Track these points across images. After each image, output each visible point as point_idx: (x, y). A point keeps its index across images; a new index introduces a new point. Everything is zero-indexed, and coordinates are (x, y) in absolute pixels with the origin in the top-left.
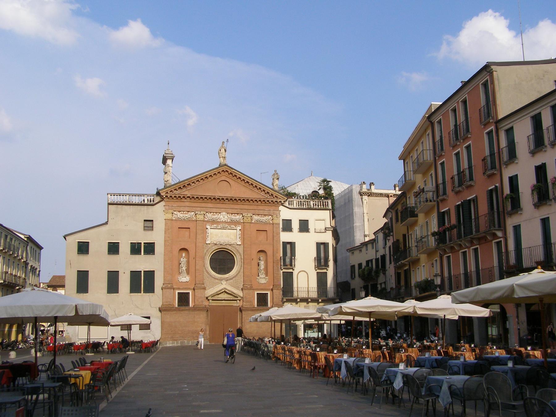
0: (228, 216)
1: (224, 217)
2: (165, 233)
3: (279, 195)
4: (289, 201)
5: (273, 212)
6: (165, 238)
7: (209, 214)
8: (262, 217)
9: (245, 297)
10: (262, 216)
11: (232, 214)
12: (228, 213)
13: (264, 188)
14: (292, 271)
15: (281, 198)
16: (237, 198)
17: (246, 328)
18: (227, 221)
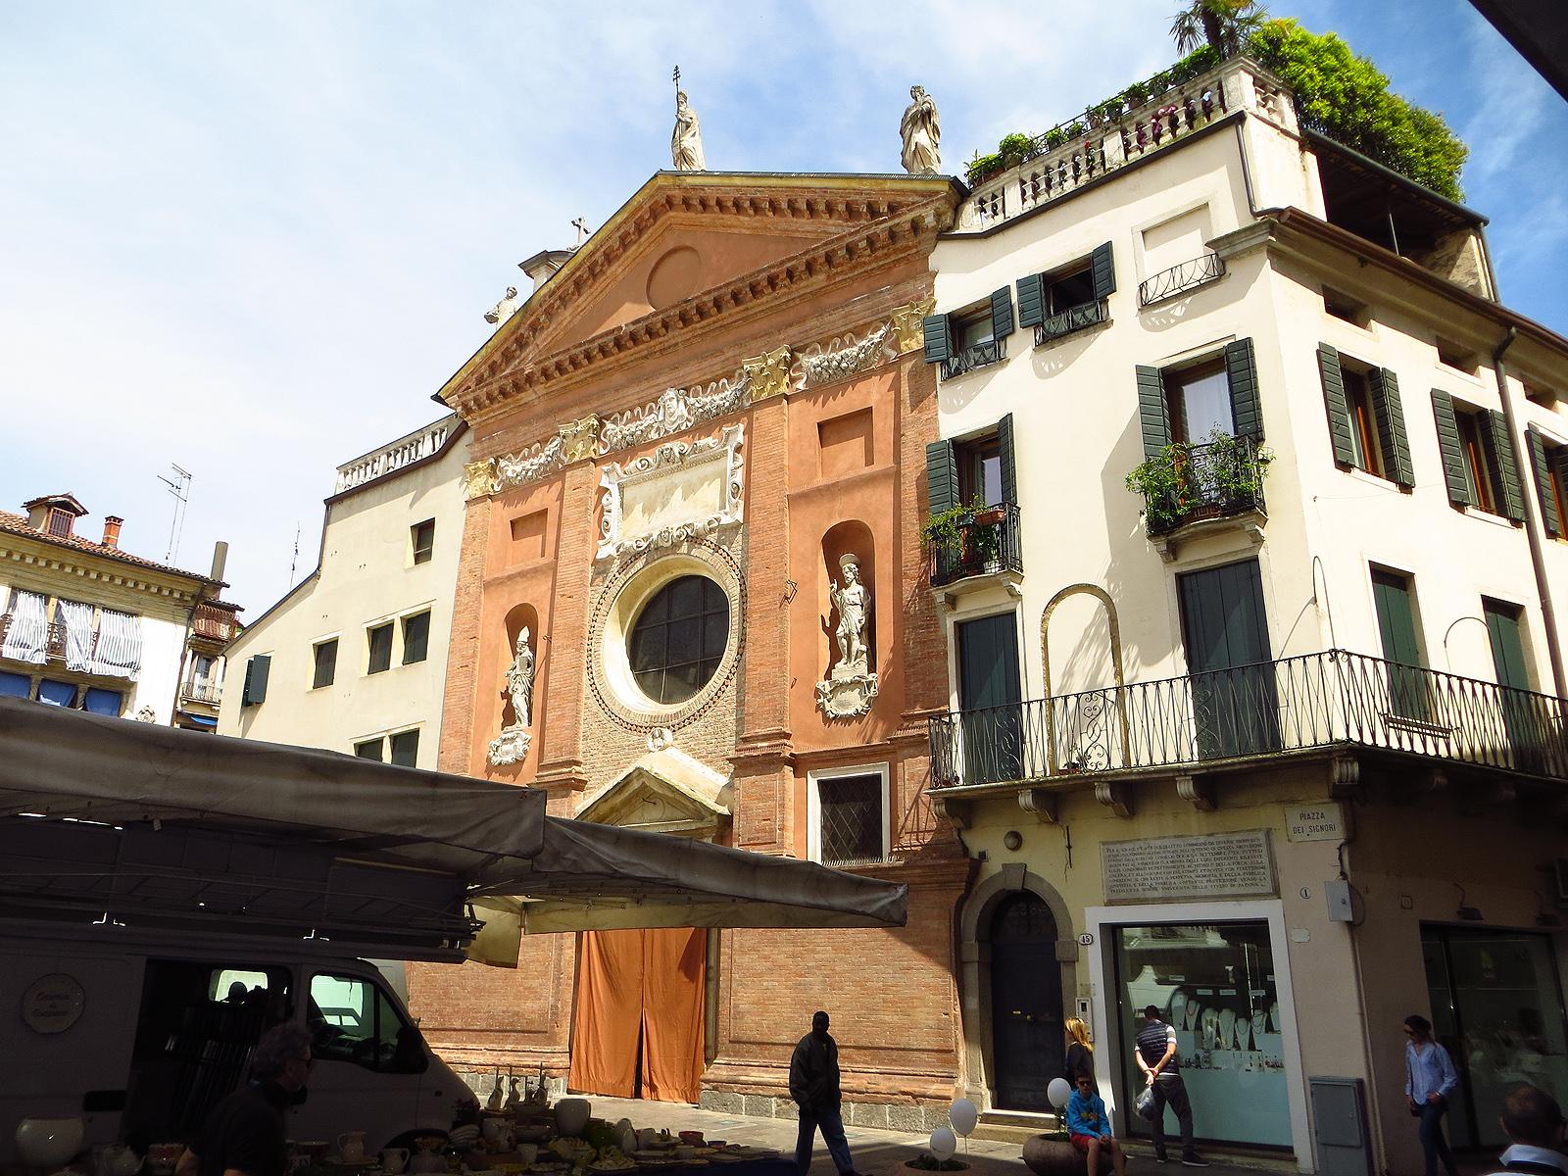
0: (691, 400)
1: (675, 408)
2: (462, 559)
3: (903, 192)
4: (982, 202)
5: (898, 297)
6: (459, 580)
7: (614, 422)
8: (843, 346)
9: (745, 810)
10: (843, 341)
11: (705, 385)
12: (687, 389)
13: (825, 190)
14: (1010, 607)
15: (917, 199)
16: (705, 299)
17: (736, 1006)
18: (683, 428)
